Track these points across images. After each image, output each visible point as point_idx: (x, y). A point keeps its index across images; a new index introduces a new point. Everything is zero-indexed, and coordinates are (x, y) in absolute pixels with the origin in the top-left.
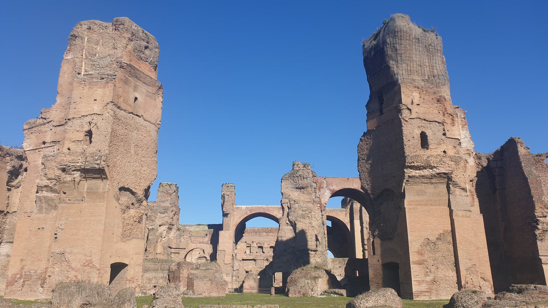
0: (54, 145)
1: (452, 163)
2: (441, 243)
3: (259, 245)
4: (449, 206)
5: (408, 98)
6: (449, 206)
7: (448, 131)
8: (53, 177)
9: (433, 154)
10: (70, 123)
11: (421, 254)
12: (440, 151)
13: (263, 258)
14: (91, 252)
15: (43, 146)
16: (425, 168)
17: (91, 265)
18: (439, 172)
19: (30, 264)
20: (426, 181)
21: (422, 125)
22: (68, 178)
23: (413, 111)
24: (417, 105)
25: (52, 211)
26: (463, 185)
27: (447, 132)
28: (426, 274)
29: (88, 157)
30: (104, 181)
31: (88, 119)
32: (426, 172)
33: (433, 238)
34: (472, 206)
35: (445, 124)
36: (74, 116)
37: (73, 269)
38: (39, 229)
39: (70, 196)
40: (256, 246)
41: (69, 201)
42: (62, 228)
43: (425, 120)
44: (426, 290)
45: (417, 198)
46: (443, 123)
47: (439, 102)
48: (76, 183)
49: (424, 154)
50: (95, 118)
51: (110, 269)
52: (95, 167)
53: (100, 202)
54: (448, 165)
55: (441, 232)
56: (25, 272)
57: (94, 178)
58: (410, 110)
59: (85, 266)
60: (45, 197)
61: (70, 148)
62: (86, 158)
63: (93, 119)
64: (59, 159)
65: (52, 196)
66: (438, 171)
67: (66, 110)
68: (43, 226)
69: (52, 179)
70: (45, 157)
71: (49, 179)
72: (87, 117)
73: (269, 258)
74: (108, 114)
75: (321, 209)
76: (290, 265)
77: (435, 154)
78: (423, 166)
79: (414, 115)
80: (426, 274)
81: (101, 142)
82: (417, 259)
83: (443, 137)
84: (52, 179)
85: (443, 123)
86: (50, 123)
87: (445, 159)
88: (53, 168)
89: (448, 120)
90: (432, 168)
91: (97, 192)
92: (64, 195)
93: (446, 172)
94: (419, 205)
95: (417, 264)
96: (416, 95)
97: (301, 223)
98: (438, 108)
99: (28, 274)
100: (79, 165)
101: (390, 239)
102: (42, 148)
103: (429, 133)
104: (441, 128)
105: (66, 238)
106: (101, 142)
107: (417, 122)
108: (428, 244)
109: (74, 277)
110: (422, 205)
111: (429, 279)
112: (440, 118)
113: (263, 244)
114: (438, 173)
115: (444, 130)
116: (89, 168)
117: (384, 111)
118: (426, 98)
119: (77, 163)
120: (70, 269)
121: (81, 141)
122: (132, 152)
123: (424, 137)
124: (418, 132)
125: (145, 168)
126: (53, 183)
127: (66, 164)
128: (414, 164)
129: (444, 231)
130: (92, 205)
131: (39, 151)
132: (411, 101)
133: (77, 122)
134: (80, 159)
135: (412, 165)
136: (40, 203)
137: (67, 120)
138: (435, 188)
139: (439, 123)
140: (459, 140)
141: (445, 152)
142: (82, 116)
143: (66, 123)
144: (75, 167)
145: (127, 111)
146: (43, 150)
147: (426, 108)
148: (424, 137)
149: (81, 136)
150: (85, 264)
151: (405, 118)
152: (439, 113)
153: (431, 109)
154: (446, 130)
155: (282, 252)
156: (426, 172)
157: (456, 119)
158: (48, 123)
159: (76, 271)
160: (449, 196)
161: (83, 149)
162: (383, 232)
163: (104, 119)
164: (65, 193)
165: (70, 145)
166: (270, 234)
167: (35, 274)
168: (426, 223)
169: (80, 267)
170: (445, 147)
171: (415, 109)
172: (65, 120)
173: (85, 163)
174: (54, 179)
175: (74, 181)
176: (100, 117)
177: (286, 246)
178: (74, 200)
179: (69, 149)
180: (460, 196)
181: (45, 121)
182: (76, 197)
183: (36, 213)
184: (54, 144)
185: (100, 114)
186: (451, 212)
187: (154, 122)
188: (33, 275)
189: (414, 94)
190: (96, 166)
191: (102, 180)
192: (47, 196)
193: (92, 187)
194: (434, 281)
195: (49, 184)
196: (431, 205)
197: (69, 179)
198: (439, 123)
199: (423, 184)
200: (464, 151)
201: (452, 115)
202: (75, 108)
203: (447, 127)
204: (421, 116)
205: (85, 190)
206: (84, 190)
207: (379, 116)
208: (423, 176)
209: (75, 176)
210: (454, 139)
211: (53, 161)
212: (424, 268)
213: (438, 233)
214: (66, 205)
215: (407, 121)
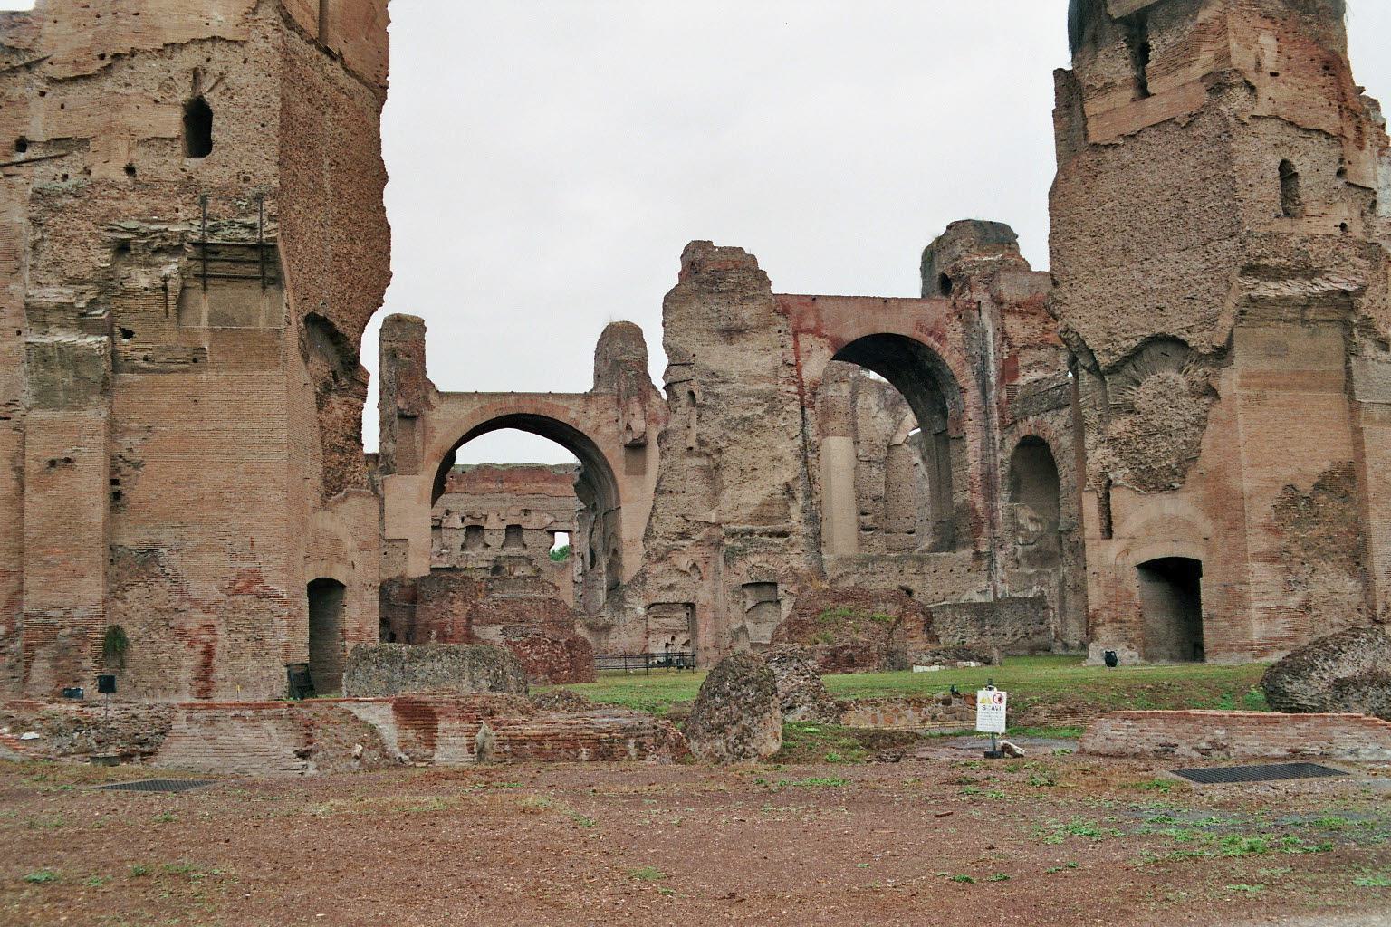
0: (63, 152)
1: (1361, 262)
2: (1324, 497)
3: (469, 521)
5: (1248, 52)
7: (1350, 163)
8: (86, 271)
9: (1313, 232)
10: (123, 72)
11: (1278, 532)
12: (1331, 224)
13: (486, 564)
14: (252, 545)
15: (21, 156)
16: (1291, 274)
17: (257, 587)
18: (1331, 288)
19: (41, 588)
20: (1290, 315)
21: (1285, 138)
22: (142, 279)
24: (1274, 74)
25: (95, 399)
27: (1350, 170)
28: (1288, 589)
29: (211, 201)
30: (271, 289)
31: (191, 58)
32: (1293, 289)
33: (1305, 486)
35: (1344, 141)
36: (137, 43)
37: (196, 603)
38: (53, 463)
39: (150, 346)
40: (459, 524)
41: (145, 365)
42: (138, 459)
43: (1292, 124)
44: (1286, 634)
45: (1265, 366)
46: (1339, 138)
47: (1326, 72)
48: (170, 296)
50: (217, 55)
51: (307, 600)
52: (242, 240)
53: (263, 367)
54: (1354, 266)
55: (1326, 466)
56: (26, 614)
57: (231, 278)
58: (1253, 89)
59: (238, 592)
60: (60, 348)
61: (135, 166)
62: (204, 201)
63: (209, 60)
64: (101, 206)
65: (89, 344)
66: (1328, 286)
67: (98, 21)
68: (68, 453)
69: (83, 282)
70: (39, 195)
71: (73, 281)
72: (184, 52)
73: (503, 565)
74: (262, 43)
75: (802, 400)
76: (701, 579)
77: (1320, 232)
78: (1288, 268)
79: (1263, 108)
80: (1288, 589)
81: (250, 147)
82: (1265, 546)
83: (1340, 183)
84: (83, 282)
85: (1339, 138)
86: (37, 70)
87: (1346, 251)
88: (82, 239)
90: (1310, 273)
91: (249, 330)
92: (126, 340)
93: (1349, 289)
94: (1271, 386)
95: (1266, 561)
96: (1268, 41)
97: (739, 448)
98: (1326, 90)
99: (35, 621)
100: (177, 229)
101: (1171, 488)
102: (19, 164)
103: (1301, 165)
104: (1332, 152)
105: (154, 497)
106: (250, 147)
107: (1270, 130)
108: (1294, 501)
109: (204, 631)
110: (1278, 387)
111: (1293, 601)
112: (1331, 122)
113: (483, 520)
114: (1328, 291)
115: (1341, 161)
116: (219, 242)
118: (1295, 53)
119: (173, 221)
120: (187, 605)
121: (172, 140)
122: (327, 186)
123: (1287, 173)
124: (1274, 161)
125: (359, 248)
126: (89, 296)
127: (133, 224)
128: (1266, 262)
129: (1334, 463)
130: (235, 378)
131: (8, 175)
132: (1253, 60)
133: (151, 69)
134: (180, 207)
135: (1261, 263)
136: (42, 370)
137: (108, 57)
138: (1311, 336)
139: (1328, 136)
140: (1375, 193)
141: (1343, 226)
142: (165, 45)
143: (104, 68)
144: (164, 238)
145: (304, 34)
146: (25, 170)
147: (1295, 88)
148: (1287, 173)
149: (171, 122)
150: (237, 586)
151: (1240, 115)
152: (1330, 105)
153: (1309, 91)
154: (1346, 161)
155: (673, 541)
156: (1293, 289)
157: (1367, 128)
158: (28, 66)
159: (207, 611)
160: (1348, 361)
161: (183, 170)
162: (1142, 467)
163: (251, 59)
164: (128, 334)
165: (134, 155)
166: (506, 485)
167: (67, 623)
168: (1288, 441)
169: (221, 596)
170: (1346, 213)
171: (1267, 89)
172: (102, 57)
173: (204, 223)
174: (88, 282)
175: (165, 288)
176: (236, 56)
177: (688, 521)
178: (164, 359)
179: (130, 170)
180: (1376, 363)
181: (16, 62)
182: (169, 349)
183: (28, 406)
184: (63, 148)
185: (236, 42)
186: (1354, 407)
187: (370, 77)
188: (58, 626)
189: (1262, 39)
190: (246, 236)
191: (264, 288)
192: (73, 346)
193: (229, 312)
194: (1305, 608)
195: (73, 300)
196: (1304, 387)
197: (144, 282)
198: (1328, 136)
199: (1281, 324)
200: (1383, 229)
201: (1357, 116)
202: (137, 14)
204: (1283, 111)
205: (204, 324)
206: (199, 324)
207: (1133, 100)
208: (1285, 301)
209: (166, 271)
210: (1362, 188)
211: (77, 215)
212: (1282, 571)
213: (1319, 471)
214: (137, 378)
215: (1244, 124)
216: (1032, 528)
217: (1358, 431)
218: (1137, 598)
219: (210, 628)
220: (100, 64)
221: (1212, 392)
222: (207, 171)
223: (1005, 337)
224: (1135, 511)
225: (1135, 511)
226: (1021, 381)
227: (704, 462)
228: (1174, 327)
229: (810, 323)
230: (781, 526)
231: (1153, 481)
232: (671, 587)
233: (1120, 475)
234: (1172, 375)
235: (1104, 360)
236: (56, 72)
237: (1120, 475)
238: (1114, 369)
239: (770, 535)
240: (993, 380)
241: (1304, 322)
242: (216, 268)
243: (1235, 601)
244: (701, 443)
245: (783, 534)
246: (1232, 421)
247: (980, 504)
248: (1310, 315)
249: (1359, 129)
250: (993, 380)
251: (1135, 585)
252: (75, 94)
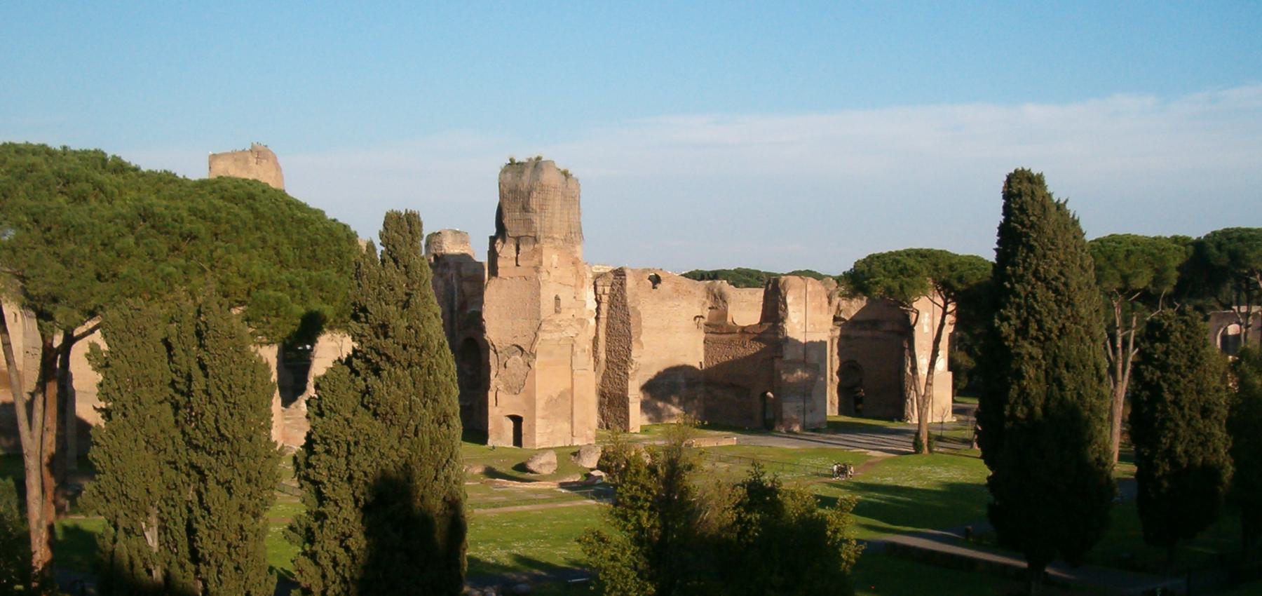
4: (571, 365)
6: (571, 365)
27: (577, 297)
33: (555, 396)
34: (588, 365)
58: (549, 273)
66: (566, 335)
96: (555, 257)
101: (515, 394)
111: (549, 431)
117: (519, 263)
123: (557, 298)
148: (557, 298)
171: (553, 273)
186: (572, 371)
194: (552, 432)
216: (469, 373)
217: (572, 379)
221: (529, 366)
223: (463, 292)
226: (468, 312)
231: (509, 389)
233: (501, 387)
235: (498, 349)
237: (501, 387)
240: (456, 309)
243: (532, 427)
246: (534, 376)
249: (583, 282)
250: (456, 309)
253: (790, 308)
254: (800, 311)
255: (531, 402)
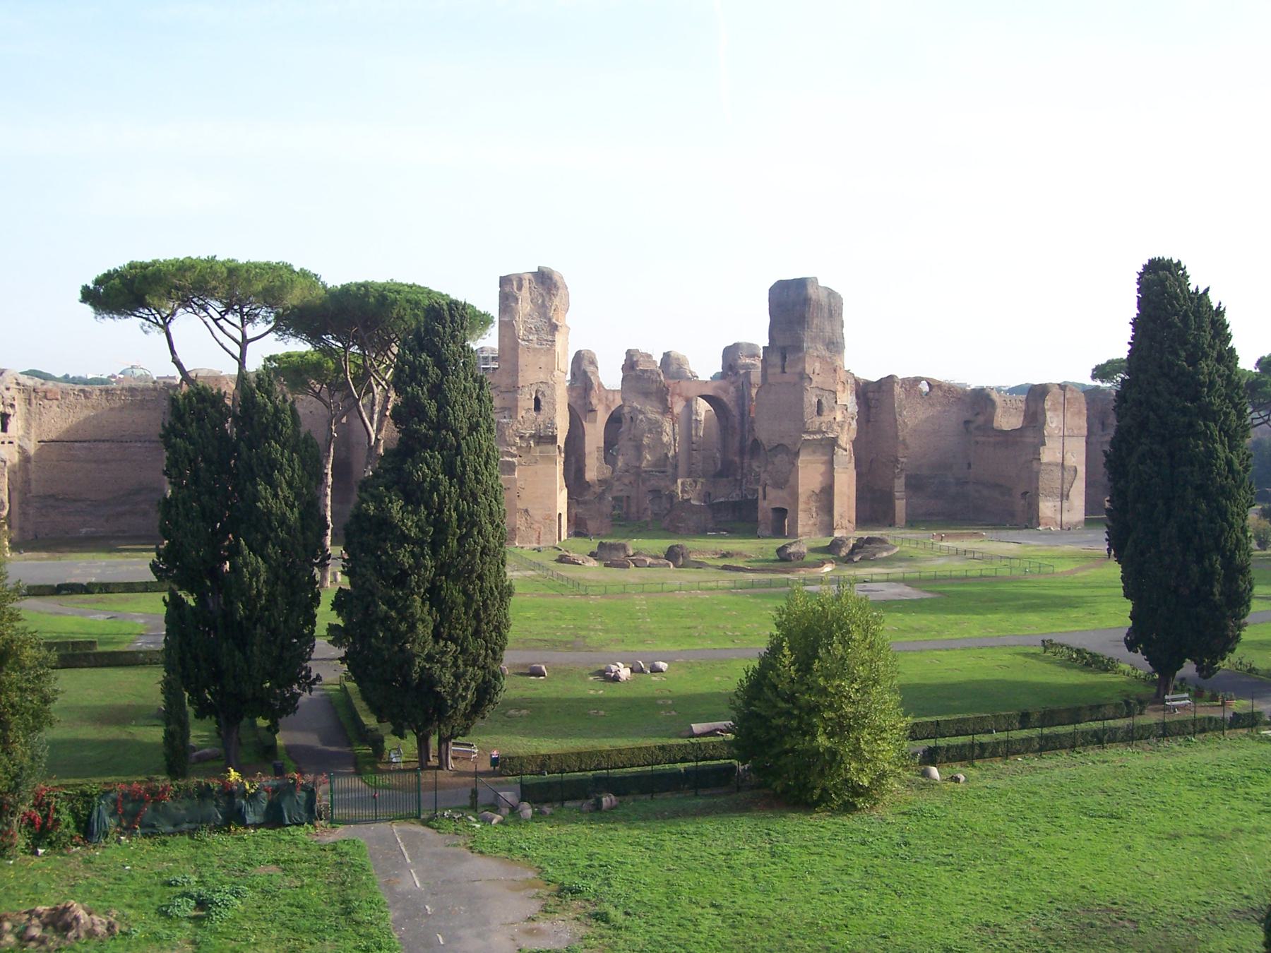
23: (814, 382)
26: (844, 446)
49: (817, 420)
89: (840, 388)
96: (817, 365)
103: (824, 401)
111: (810, 522)
117: (786, 370)
123: (819, 402)
124: (815, 400)
148: (819, 402)
171: (815, 378)
203: (838, 395)
218: (771, 518)
219: (540, 528)
220: (513, 389)
222: (540, 418)
224: (772, 493)
225: (772, 493)
227: (634, 443)
228: (785, 441)
229: (678, 391)
230: (663, 469)
232: (621, 490)
234: (785, 456)
236: (503, 389)
238: (770, 451)
239: (659, 472)
241: (821, 445)
242: (542, 440)
244: (634, 436)
245: (663, 472)
247: (737, 459)
248: (823, 443)
251: (770, 514)
252: (506, 395)
253: (1049, 414)
254: (1058, 416)
255: (794, 496)
